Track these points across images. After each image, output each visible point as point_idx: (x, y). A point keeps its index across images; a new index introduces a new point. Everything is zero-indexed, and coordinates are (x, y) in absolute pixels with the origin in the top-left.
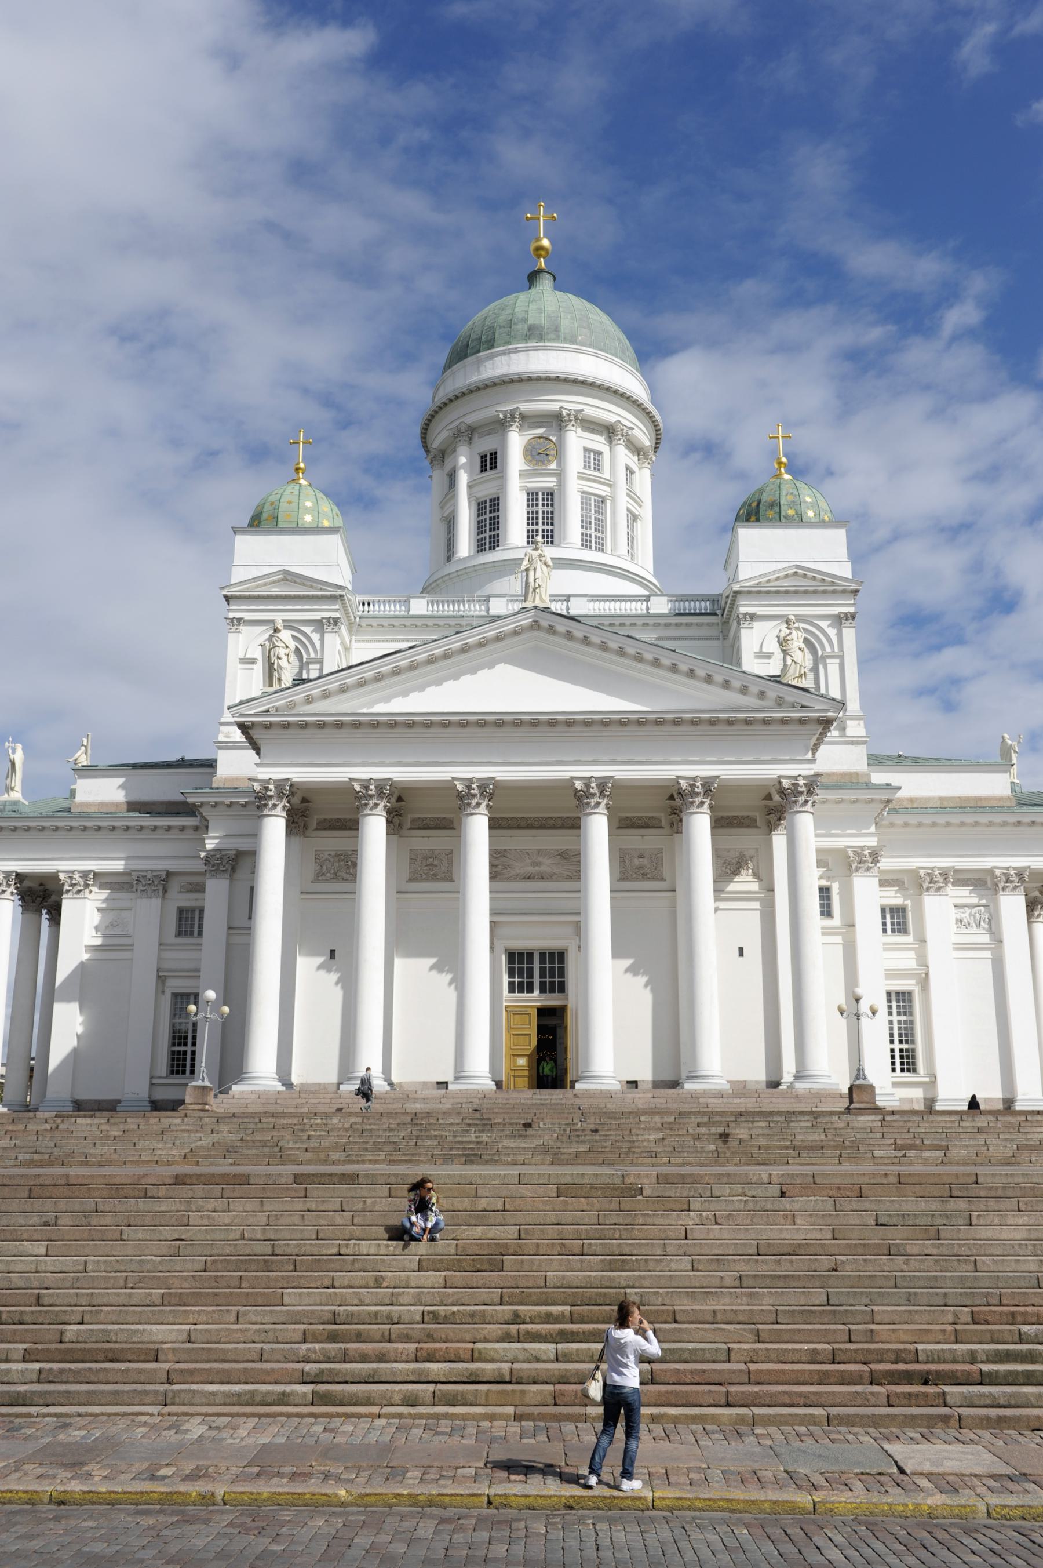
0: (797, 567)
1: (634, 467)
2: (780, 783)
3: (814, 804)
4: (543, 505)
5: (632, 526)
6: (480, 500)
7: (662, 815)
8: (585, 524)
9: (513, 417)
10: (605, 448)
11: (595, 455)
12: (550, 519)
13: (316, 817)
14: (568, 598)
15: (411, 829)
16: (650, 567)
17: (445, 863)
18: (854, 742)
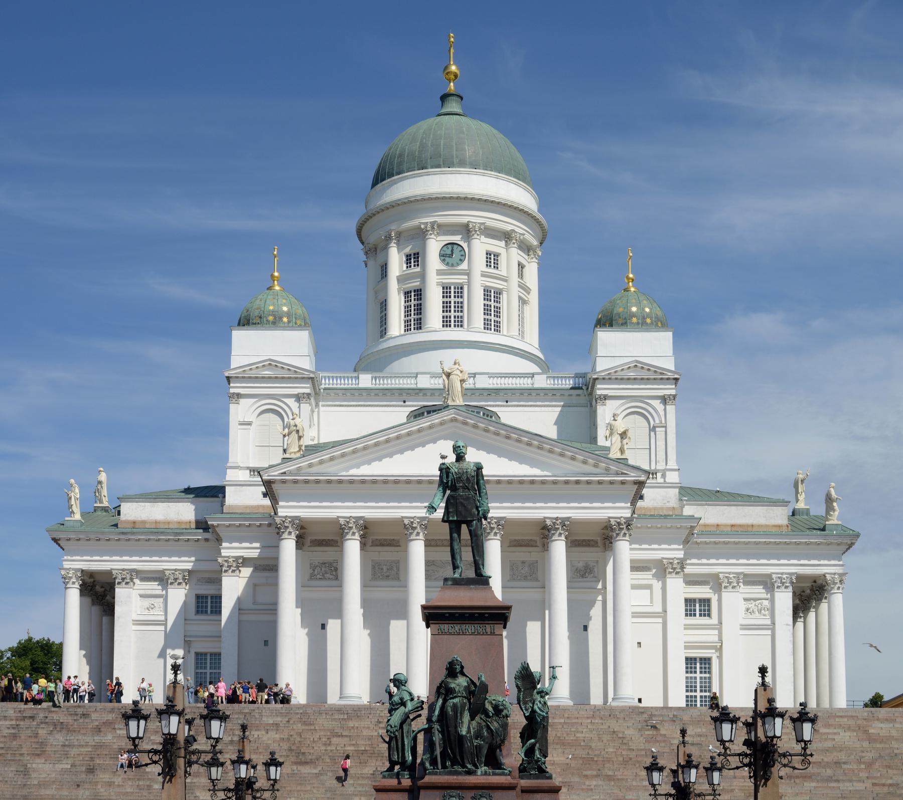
0: (637, 362)
1: (524, 262)
2: (610, 521)
3: (630, 535)
4: (455, 297)
5: (523, 308)
6: (406, 291)
7: (538, 539)
8: (487, 310)
9: (433, 228)
10: (503, 252)
11: (494, 256)
12: (460, 307)
13: (309, 538)
15: (372, 546)
16: (536, 343)
17: (395, 569)
18: (672, 486)
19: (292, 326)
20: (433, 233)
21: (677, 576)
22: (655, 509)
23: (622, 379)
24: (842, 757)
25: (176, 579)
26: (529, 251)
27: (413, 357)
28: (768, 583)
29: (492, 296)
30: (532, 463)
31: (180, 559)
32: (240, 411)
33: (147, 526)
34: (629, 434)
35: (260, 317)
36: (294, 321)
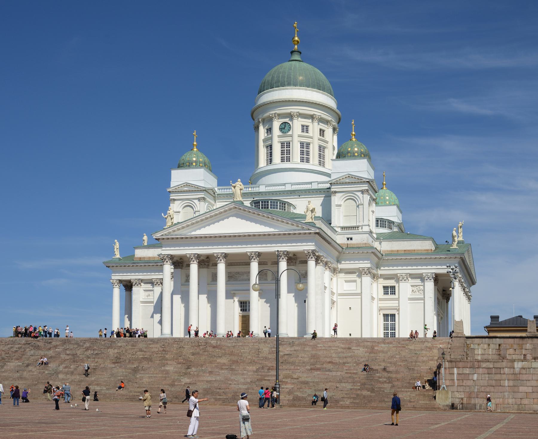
8: (302, 153)
13: (185, 263)
14: (284, 185)
15: (212, 266)
19: (198, 167)
20: (276, 118)
21: (367, 276)
22: (357, 244)
23: (343, 183)
24: (349, 360)
25: (157, 283)
26: (327, 123)
27: (267, 177)
28: (421, 277)
29: (305, 147)
30: (270, 226)
31: (147, 274)
32: (175, 207)
33: (146, 259)
34: (316, 210)
35: (184, 164)
36: (198, 164)
